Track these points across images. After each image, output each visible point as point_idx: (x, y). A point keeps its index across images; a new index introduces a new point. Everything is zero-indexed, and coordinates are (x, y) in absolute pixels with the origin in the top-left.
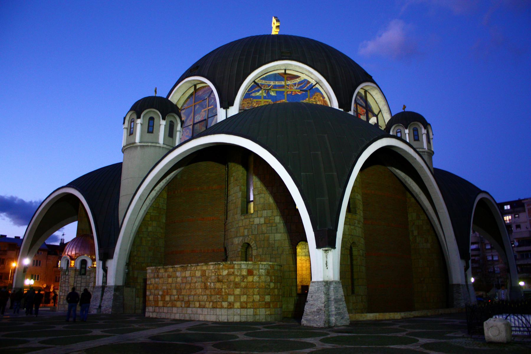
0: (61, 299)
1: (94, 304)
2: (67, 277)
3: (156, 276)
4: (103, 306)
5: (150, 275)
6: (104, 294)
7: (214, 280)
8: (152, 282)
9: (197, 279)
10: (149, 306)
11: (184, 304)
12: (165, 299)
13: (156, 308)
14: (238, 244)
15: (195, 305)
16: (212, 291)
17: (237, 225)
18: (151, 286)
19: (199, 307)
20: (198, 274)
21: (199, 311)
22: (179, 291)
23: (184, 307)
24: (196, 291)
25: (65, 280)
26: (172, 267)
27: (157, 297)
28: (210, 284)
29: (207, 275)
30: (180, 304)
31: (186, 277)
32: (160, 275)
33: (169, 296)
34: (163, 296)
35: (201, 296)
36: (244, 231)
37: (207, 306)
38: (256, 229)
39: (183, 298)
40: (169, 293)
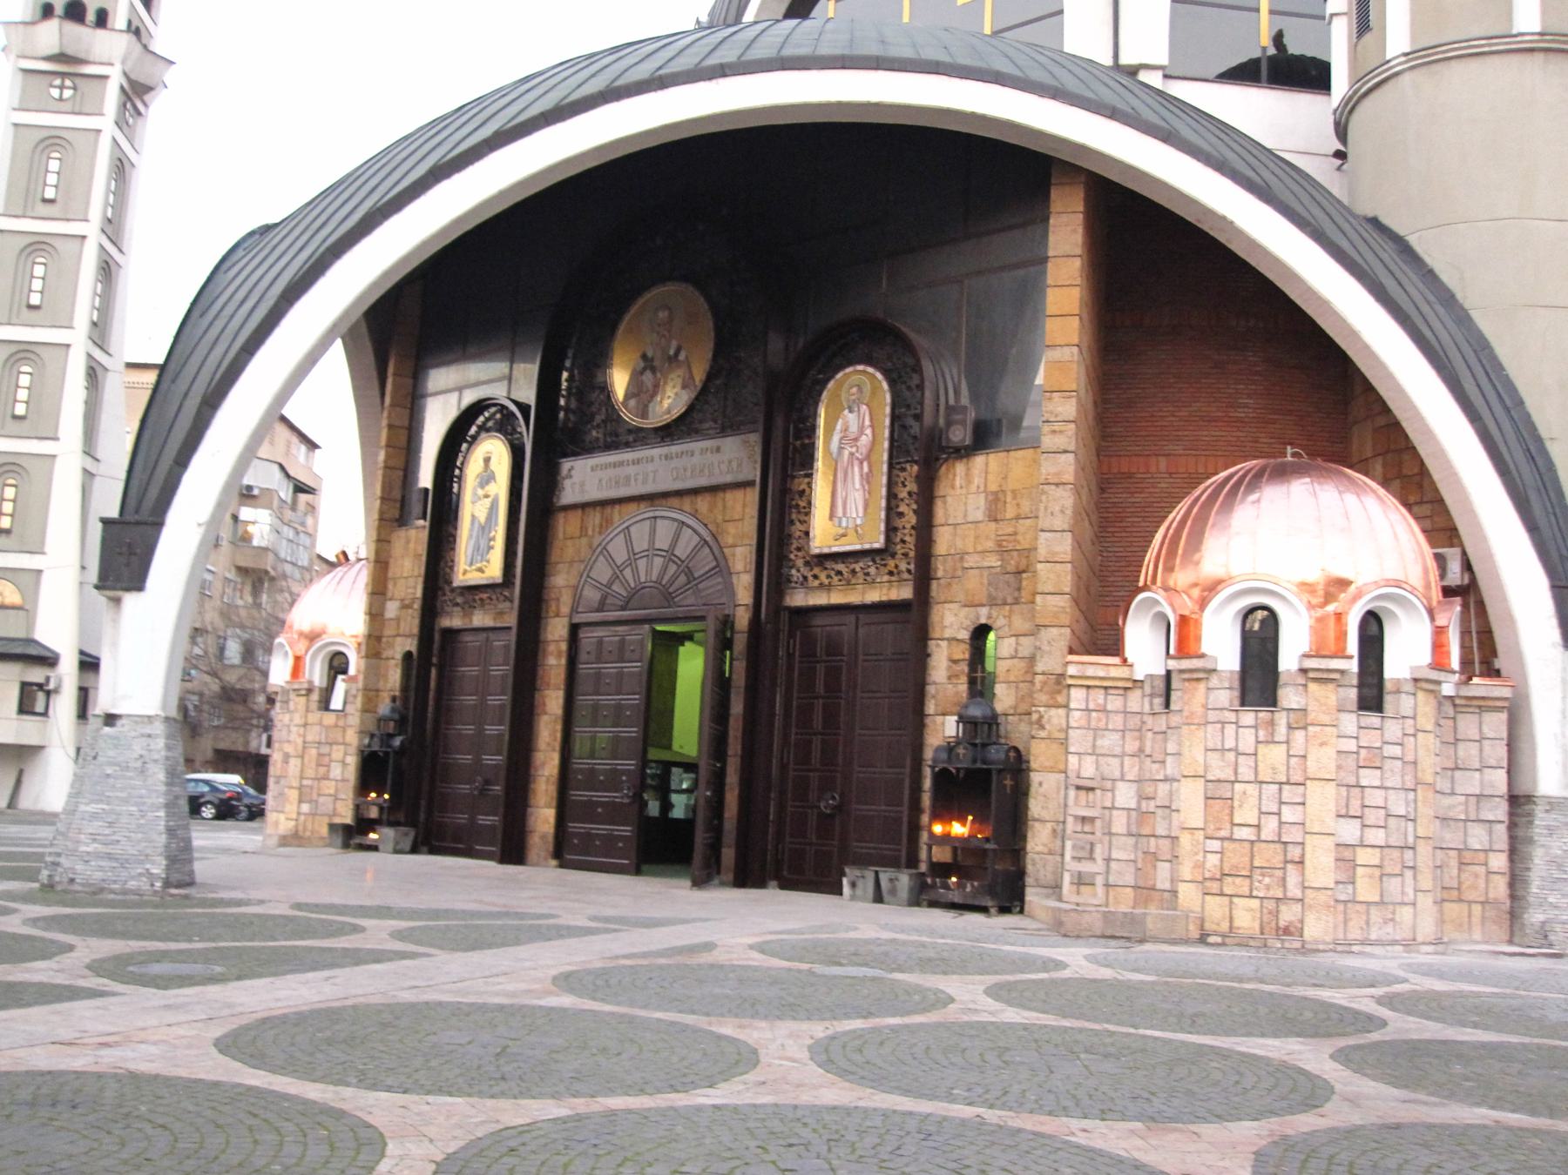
0: (1360, 871)
2: (1393, 729)
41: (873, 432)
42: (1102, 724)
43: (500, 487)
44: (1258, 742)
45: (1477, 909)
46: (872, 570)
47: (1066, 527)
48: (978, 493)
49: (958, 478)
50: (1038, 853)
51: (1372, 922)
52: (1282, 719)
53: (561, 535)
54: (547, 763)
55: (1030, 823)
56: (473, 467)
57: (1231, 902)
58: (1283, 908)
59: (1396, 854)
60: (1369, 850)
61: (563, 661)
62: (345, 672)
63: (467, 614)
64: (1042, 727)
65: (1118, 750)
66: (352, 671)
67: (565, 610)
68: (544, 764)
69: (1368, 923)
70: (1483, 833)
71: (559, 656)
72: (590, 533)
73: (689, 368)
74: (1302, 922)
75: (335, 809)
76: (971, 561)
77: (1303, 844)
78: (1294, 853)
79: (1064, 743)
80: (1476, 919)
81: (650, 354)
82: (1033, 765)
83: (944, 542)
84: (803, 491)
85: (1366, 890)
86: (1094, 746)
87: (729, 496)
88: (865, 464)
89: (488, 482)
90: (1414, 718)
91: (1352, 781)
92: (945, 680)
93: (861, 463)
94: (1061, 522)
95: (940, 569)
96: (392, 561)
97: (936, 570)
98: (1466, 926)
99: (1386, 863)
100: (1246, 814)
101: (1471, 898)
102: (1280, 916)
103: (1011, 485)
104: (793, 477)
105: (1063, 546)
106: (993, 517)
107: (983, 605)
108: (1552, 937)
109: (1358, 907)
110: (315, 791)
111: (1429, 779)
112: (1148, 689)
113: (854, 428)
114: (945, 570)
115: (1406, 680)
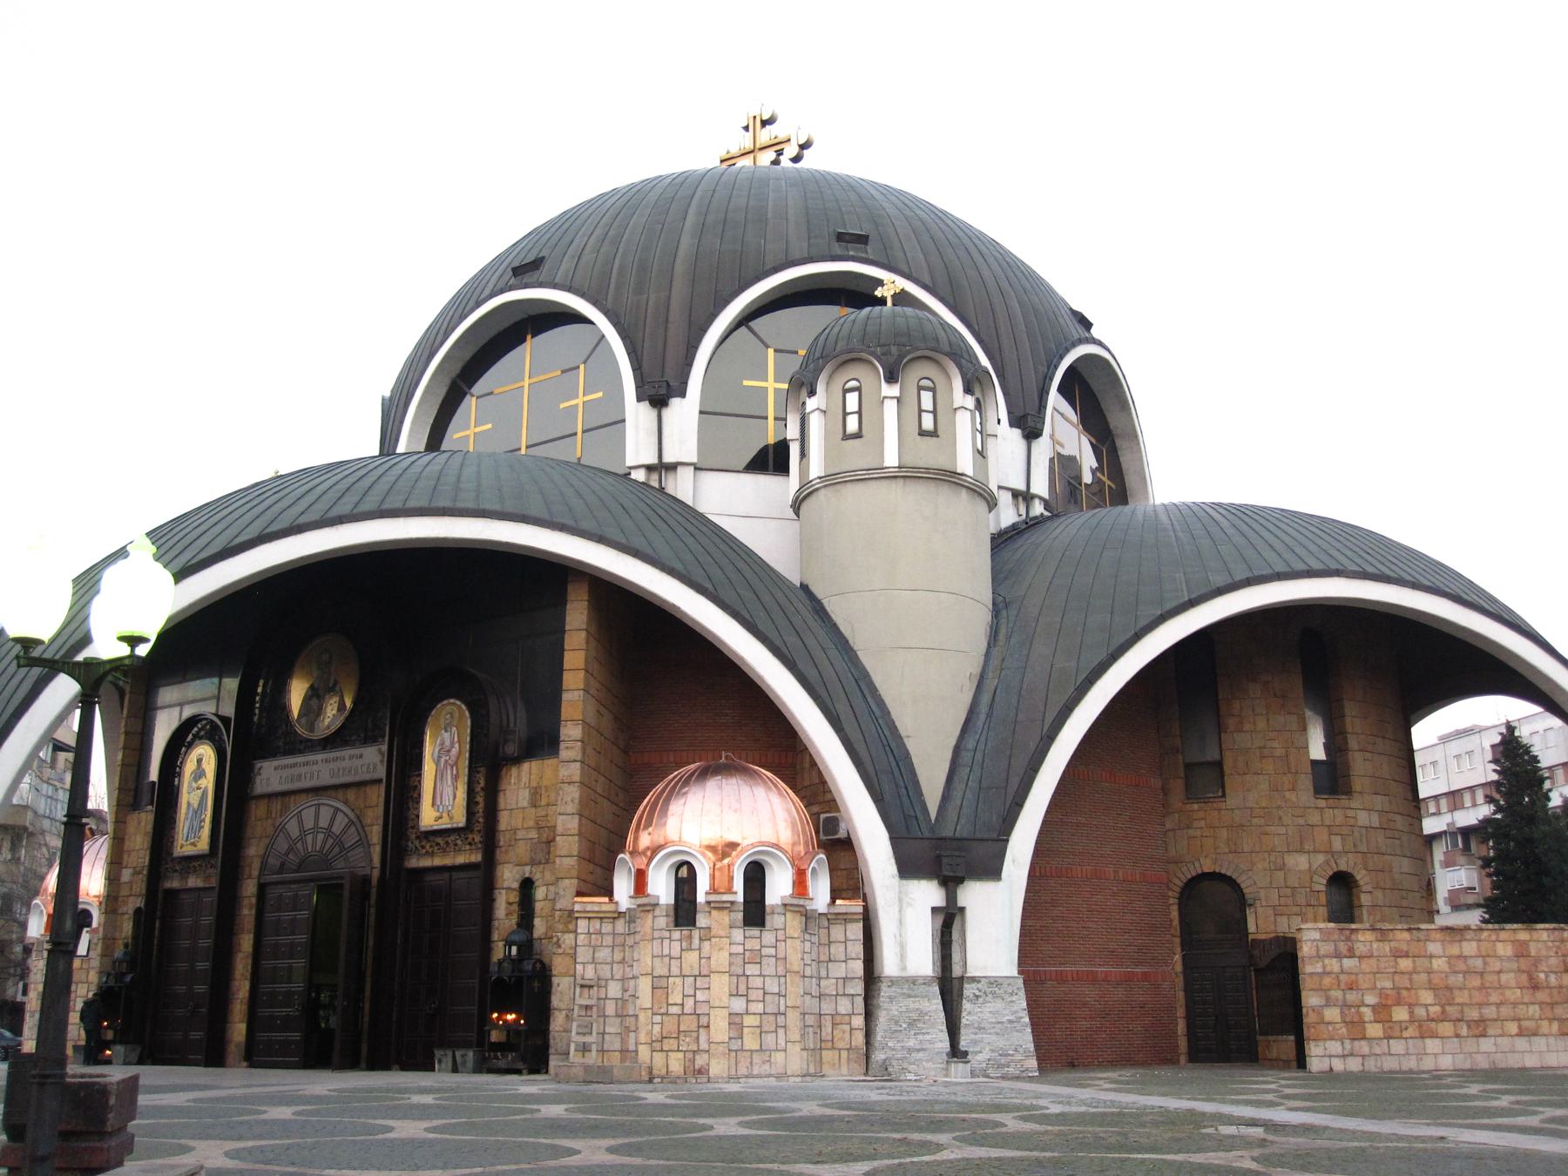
0: (745, 1030)
1: (911, 1043)
2: (768, 937)
3: (1343, 947)
4: (980, 1052)
5: (1317, 946)
6: (966, 1005)
7: (1557, 967)
8: (1328, 969)
9: (1504, 964)
10: (1325, 1040)
11: (1465, 1027)
12: (1391, 1016)
13: (1356, 1043)
14: (1311, 872)
15: (1502, 1029)
16: (1555, 991)
17: (1301, 821)
18: (1327, 981)
19: (1520, 1034)
20: (1505, 950)
21: (1521, 1043)
22: (1444, 992)
23: (1468, 1037)
24: (1503, 994)
25: (760, 950)
26: (1409, 930)
27: (1358, 1012)
28: (1546, 978)
29: (1533, 953)
30: (1452, 1028)
31: (1460, 957)
32: (1361, 948)
33: (1407, 1007)
34: (1382, 1011)
35: (1521, 1007)
36: (1330, 842)
37: (1545, 1030)
38: (1364, 840)
39: (1462, 1011)
40: (1407, 1000)
41: (460, 746)
42: (599, 943)
43: (209, 782)
44: (682, 950)
45: (844, 1054)
46: (459, 842)
47: (574, 811)
48: (525, 788)
49: (513, 778)
50: (558, 1032)
51: (754, 1062)
52: (696, 934)
53: (253, 819)
54: (241, 989)
55: (552, 1012)
56: (190, 766)
57: (667, 1055)
58: (697, 1057)
59: (772, 1018)
60: (752, 1016)
61: (254, 912)
62: (89, 925)
63: (184, 878)
64: (560, 947)
65: (609, 960)
66: (95, 924)
67: (255, 873)
68: (238, 990)
69: (751, 1063)
70: (848, 1003)
72: (274, 815)
74: (708, 1065)
76: (520, 835)
77: (709, 1014)
78: (704, 1020)
79: (574, 957)
80: (844, 1060)
81: (316, 686)
82: (554, 972)
83: (504, 821)
84: (416, 786)
85: (750, 1042)
86: (593, 958)
87: (368, 789)
88: (454, 768)
89: (200, 778)
90: (785, 929)
91: (740, 972)
92: (504, 917)
93: (452, 767)
94: (571, 808)
95: (502, 840)
96: (127, 837)
97: (499, 841)
98: (837, 1066)
99: (763, 1024)
100: (676, 998)
101: (841, 1047)
102: (696, 1063)
103: (545, 782)
104: (409, 777)
105: (573, 824)
106: (534, 804)
107: (526, 864)
108: (890, 1069)
109: (745, 1054)
111: (796, 968)
112: (627, 918)
113: (448, 743)
114: (504, 841)
115: (777, 905)
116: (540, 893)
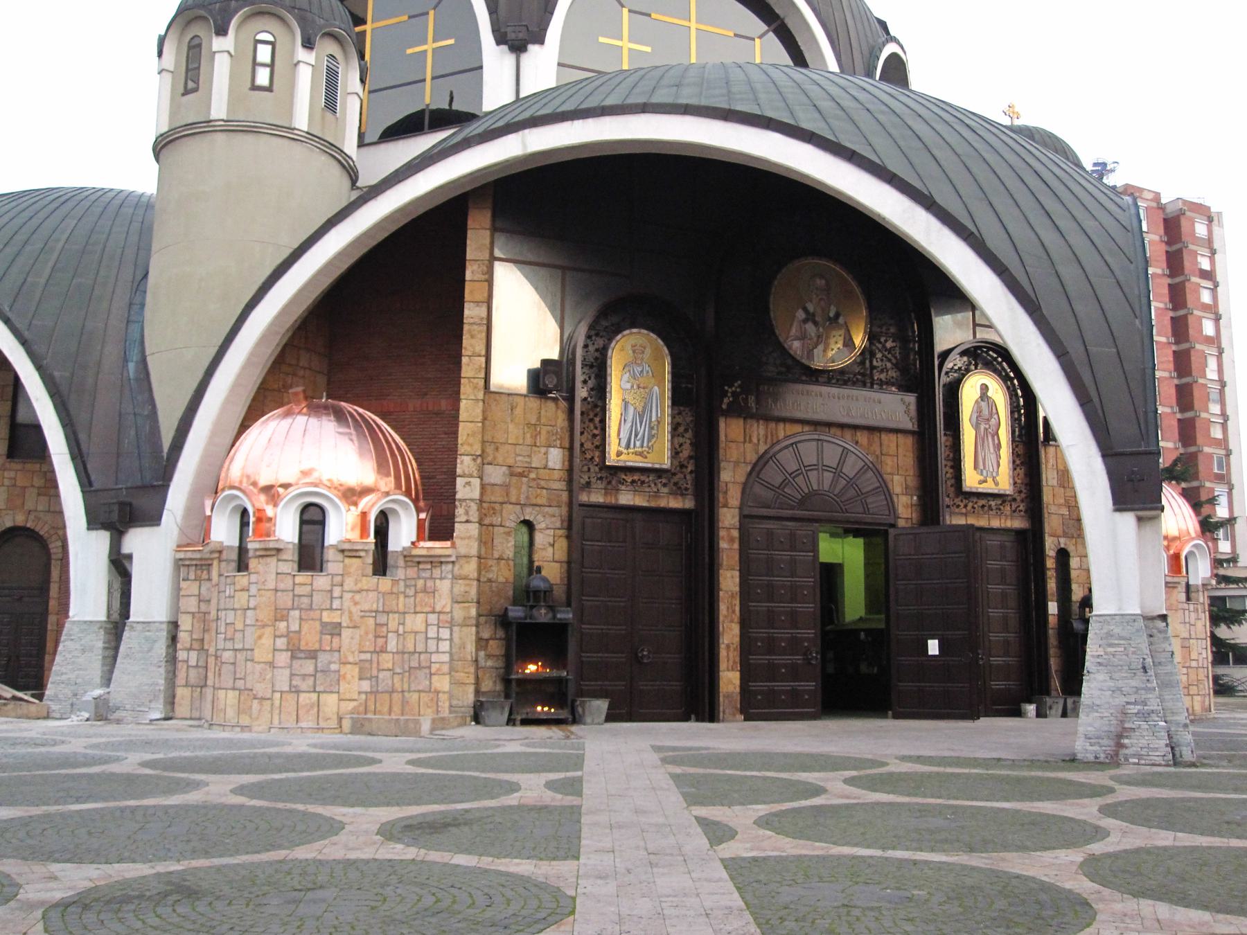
61: (736, 546)
71: (732, 540)
72: (755, 440)
73: (848, 332)
75: (393, 685)
100: (1194, 656)
110: (375, 665)
113: (986, 412)
116: (1074, 562)
